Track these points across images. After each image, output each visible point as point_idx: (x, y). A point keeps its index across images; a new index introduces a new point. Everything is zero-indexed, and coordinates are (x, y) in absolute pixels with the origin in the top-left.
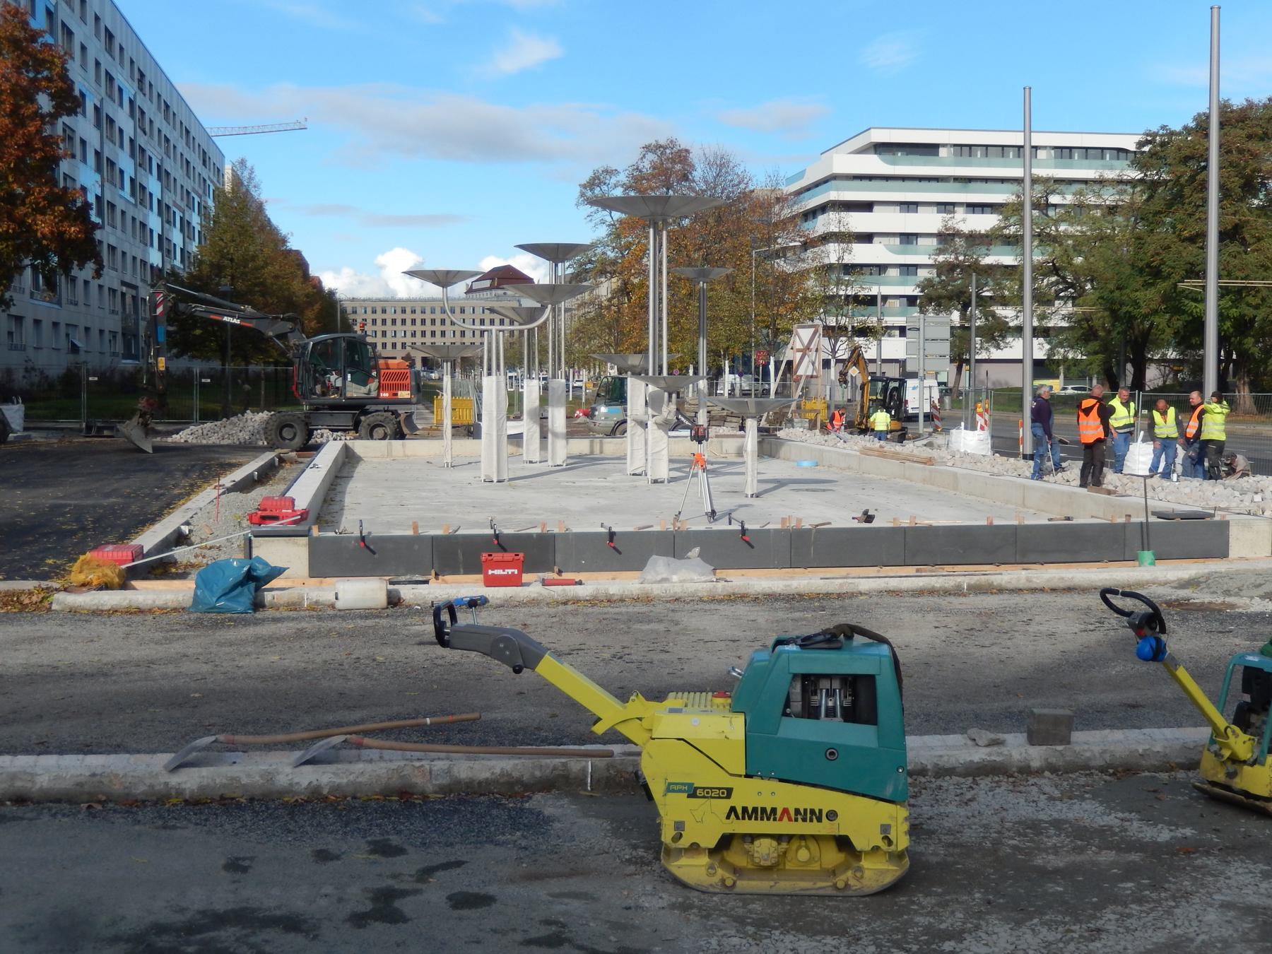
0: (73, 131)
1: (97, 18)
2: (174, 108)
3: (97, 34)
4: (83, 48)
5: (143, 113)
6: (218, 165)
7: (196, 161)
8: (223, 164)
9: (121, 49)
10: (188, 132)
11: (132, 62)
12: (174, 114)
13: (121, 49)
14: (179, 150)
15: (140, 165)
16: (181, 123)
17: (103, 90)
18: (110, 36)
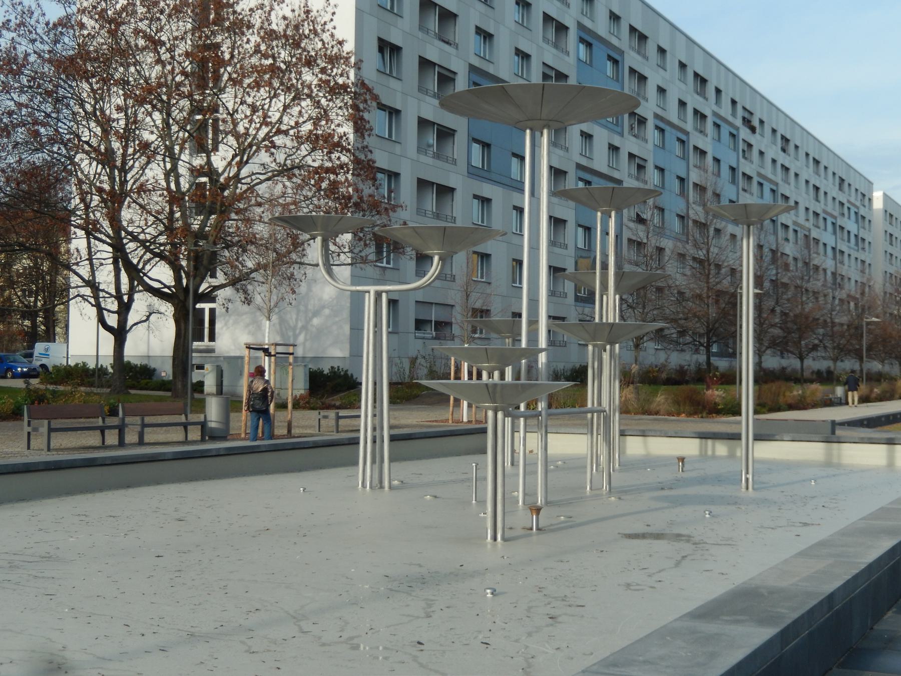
0: (646, 160)
1: (683, 66)
2: (796, 139)
3: (683, 80)
4: (661, 91)
5: (750, 146)
6: (862, 189)
7: (828, 185)
8: (871, 191)
9: (718, 91)
10: (817, 162)
11: (734, 102)
12: (797, 147)
13: (718, 91)
14: (804, 176)
15: (744, 190)
16: (807, 155)
17: (689, 125)
18: (701, 81)
